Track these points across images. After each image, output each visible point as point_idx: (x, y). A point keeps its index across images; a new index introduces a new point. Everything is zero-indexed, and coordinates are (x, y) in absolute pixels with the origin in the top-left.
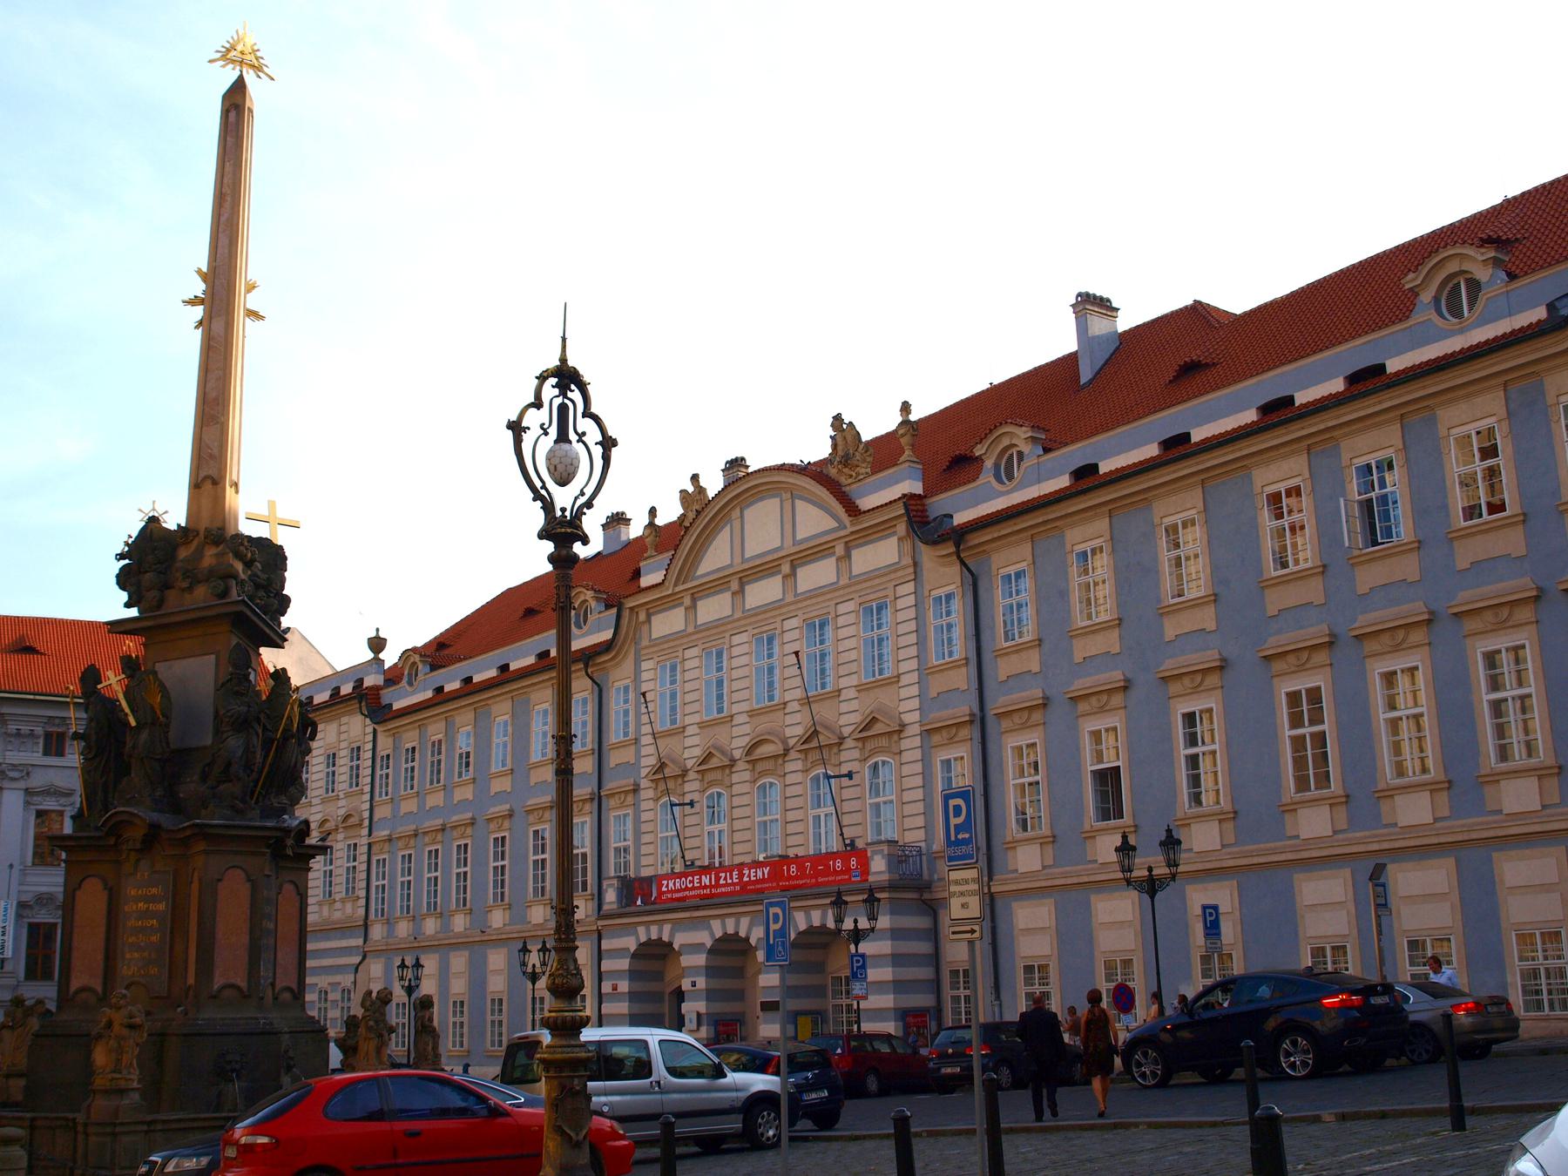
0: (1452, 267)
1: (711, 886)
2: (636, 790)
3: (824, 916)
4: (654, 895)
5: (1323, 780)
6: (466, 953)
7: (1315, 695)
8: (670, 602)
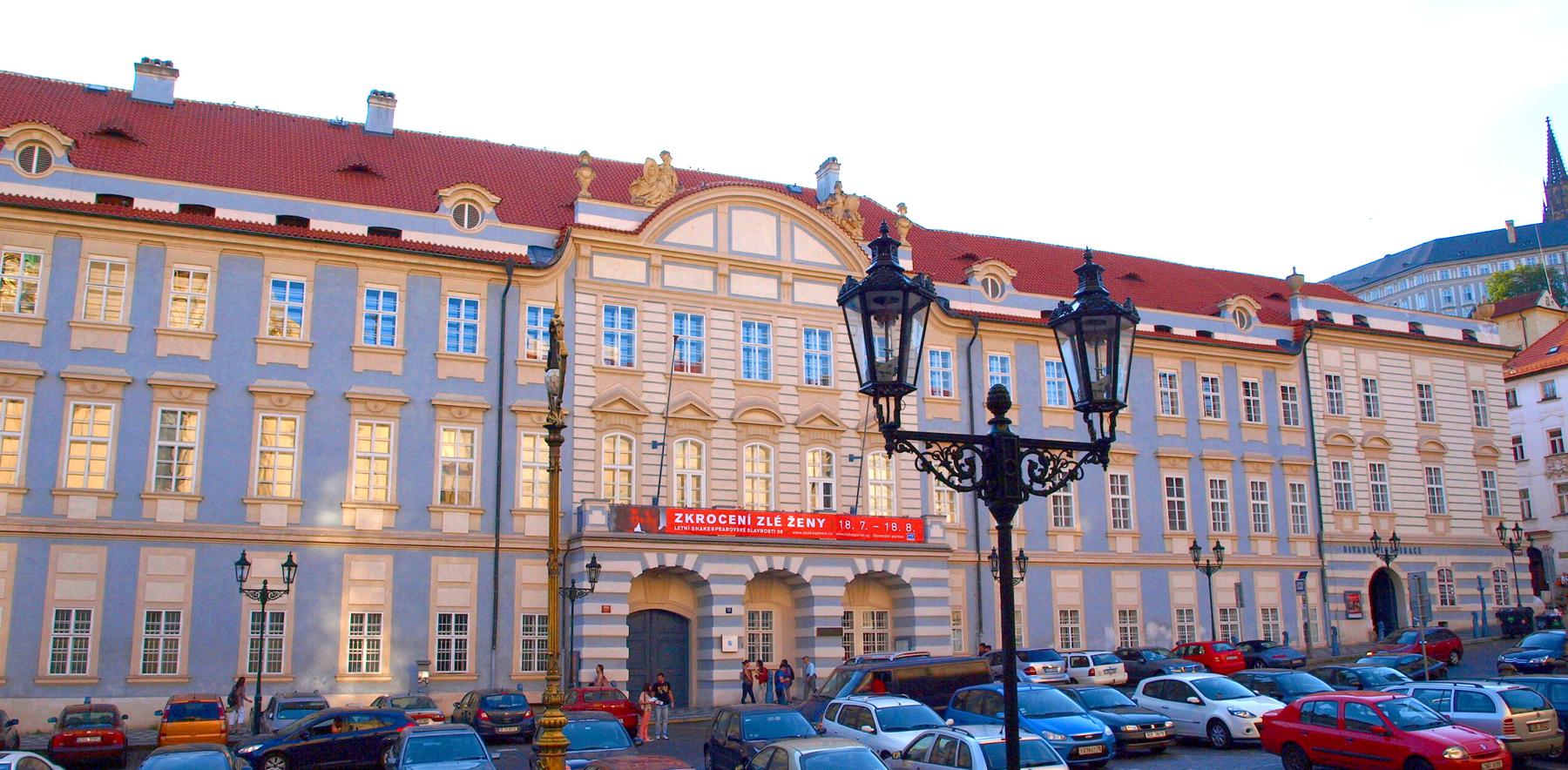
1: (747, 526)
3: (886, 564)
4: (663, 523)
5: (1183, 526)
6: (192, 552)
7: (1179, 481)
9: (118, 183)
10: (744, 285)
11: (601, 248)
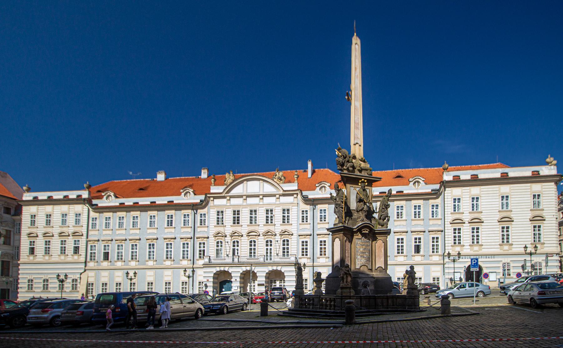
0: (417, 180)
2: (208, 238)
8: (224, 197)
9: (122, 200)
10: (250, 201)
11: (215, 198)
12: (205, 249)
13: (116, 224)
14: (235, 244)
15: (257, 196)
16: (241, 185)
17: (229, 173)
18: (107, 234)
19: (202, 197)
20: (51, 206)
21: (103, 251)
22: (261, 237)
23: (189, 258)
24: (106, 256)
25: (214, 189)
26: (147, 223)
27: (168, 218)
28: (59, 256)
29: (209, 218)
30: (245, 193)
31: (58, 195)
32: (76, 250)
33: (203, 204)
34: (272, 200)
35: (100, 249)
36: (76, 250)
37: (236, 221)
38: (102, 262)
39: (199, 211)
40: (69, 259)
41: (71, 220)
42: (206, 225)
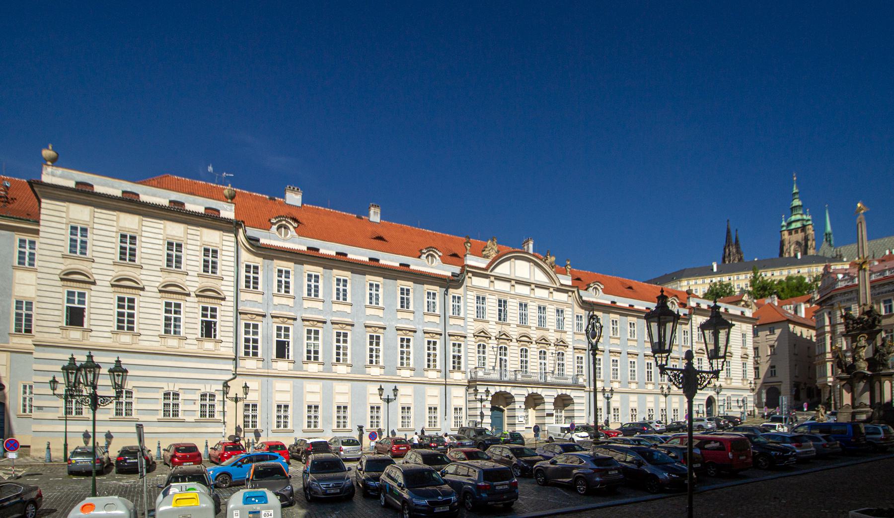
12: (462, 354)
13: (301, 287)
14: (503, 350)
15: (527, 284)
16: (508, 263)
17: (493, 240)
18: (282, 304)
19: (457, 270)
20: (136, 219)
21: (275, 339)
22: (534, 345)
23: (438, 367)
24: (282, 350)
25: (472, 261)
26: (364, 296)
27: (402, 293)
28: (160, 336)
29: (465, 303)
30: (512, 277)
31: (154, 195)
32: (208, 330)
33: (454, 282)
34: (543, 293)
35: (267, 335)
36: (208, 330)
37: (502, 315)
38: (273, 361)
39: (451, 291)
40: (191, 347)
41: (192, 259)
42: (462, 315)
